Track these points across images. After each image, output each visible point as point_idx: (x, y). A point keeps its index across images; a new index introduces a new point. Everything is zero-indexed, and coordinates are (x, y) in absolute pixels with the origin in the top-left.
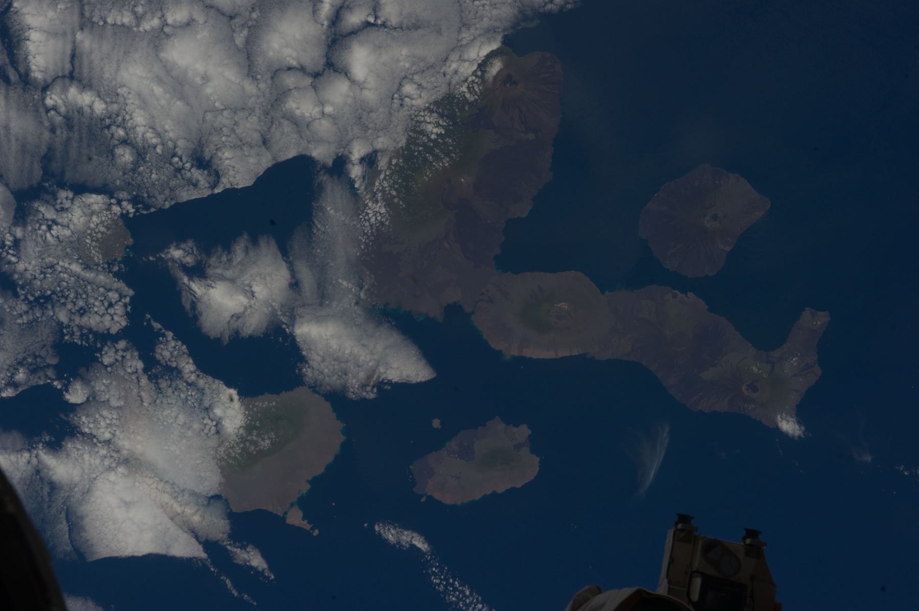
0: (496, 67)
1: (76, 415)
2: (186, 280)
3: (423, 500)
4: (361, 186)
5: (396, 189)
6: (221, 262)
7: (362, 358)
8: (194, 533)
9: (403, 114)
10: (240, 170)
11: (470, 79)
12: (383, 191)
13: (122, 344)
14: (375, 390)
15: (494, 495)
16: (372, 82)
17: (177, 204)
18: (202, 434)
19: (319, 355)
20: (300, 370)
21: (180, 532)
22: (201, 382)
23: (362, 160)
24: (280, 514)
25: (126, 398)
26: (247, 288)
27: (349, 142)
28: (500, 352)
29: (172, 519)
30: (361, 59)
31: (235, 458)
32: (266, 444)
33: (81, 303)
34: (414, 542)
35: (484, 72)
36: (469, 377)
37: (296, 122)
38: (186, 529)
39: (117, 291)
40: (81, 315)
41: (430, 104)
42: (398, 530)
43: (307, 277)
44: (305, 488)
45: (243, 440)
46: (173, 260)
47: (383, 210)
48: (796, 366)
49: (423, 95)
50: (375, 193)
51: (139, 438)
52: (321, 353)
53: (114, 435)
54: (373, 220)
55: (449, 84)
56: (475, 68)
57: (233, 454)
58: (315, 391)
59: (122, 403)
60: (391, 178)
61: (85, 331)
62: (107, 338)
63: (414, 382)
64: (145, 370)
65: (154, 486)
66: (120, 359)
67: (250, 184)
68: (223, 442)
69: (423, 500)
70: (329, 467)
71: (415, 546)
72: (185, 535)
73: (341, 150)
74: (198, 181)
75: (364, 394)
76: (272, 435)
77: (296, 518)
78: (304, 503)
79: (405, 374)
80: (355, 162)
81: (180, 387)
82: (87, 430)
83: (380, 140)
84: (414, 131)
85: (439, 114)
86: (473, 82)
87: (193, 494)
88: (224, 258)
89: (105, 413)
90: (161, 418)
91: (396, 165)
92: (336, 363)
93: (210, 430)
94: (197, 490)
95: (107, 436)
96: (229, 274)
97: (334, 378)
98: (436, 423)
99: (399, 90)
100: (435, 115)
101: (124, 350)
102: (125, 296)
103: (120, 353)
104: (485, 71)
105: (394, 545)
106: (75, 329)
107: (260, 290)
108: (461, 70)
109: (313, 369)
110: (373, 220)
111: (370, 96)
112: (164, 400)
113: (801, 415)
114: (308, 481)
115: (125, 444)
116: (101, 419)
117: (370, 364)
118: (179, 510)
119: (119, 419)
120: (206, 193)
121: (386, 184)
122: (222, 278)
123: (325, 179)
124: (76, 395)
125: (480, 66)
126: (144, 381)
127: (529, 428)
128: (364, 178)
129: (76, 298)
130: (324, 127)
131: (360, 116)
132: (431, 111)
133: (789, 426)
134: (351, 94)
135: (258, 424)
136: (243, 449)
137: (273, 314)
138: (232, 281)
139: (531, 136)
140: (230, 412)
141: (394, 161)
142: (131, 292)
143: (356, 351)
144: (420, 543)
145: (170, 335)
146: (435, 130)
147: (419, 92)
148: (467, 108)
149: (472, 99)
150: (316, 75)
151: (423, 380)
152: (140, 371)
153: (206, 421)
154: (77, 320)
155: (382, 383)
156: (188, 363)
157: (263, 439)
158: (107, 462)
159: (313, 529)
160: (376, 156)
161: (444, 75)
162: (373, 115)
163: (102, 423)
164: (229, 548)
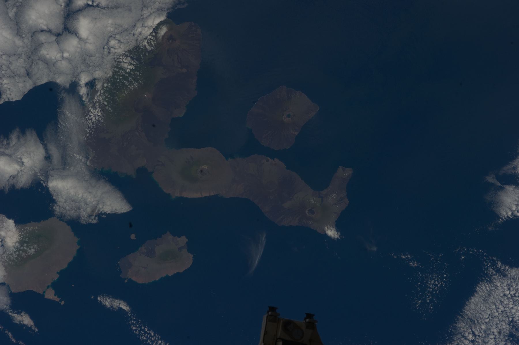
3: (126, 281)
4: (86, 99)
5: (106, 101)
9: (110, 58)
11: (149, 37)
12: (99, 102)
14: (97, 218)
15: (167, 277)
16: (91, 39)
19: (63, 198)
20: (52, 208)
23: (87, 84)
24: (41, 292)
27: (79, 74)
28: (169, 194)
32: (32, 251)
34: (121, 306)
35: (156, 33)
36: (152, 210)
37: (46, 62)
41: (126, 52)
42: (111, 299)
44: (56, 277)
47: (99, 114)
48: (335, 199)
49: (121, 46)
50: (95, 104)
52: (64, 197)
54: (94, 119)
55: (137, 40)
58: (61, 220)
60: (104, 94)
63: (120, 213)
69: (126, 281)
70: (70, 264)
71: (121, 308)
73: (74, 78)
75: (90, 220)
76: (36, 246)
77: (50, 295)
78: (55, 286)
79: (114, 209)
80: (83, 85)
83: (97, 72)
84: (117, 67)
85: (131, 57)
86: (150, 39)
91: (107, 87)
92: (73, 203)
97: (73, 212)
98: (133, 237)
99: (107, 44)
104: (157, 33)
105: (109, 308)
108: (143, 32)
109: (60, 207)
110: (94, 119)
111: (90, 47)
113: (338, 227)
114: (58, 273)
117: (94, 203)
123: (65, 95)
127: (186, 237)
128: (88, 94)
130: (64, 65)
131: (85, 59)
132: (127, 56)
133: (332, 233)
134: (79, 46)
137: (35, 174)
139: (184, 70)
141: (106, 85)
143: (85, 195)
144: (125, 307)
146: (129, 67)
147: (119, 45)
148: (147, 54)
149: (150, 49)
150: (58, 35)
151: (125, 212)
155: (101, 214)
159: (61, 301)
160: (95, 82)
161: (134, 35)
162: (92, 58)
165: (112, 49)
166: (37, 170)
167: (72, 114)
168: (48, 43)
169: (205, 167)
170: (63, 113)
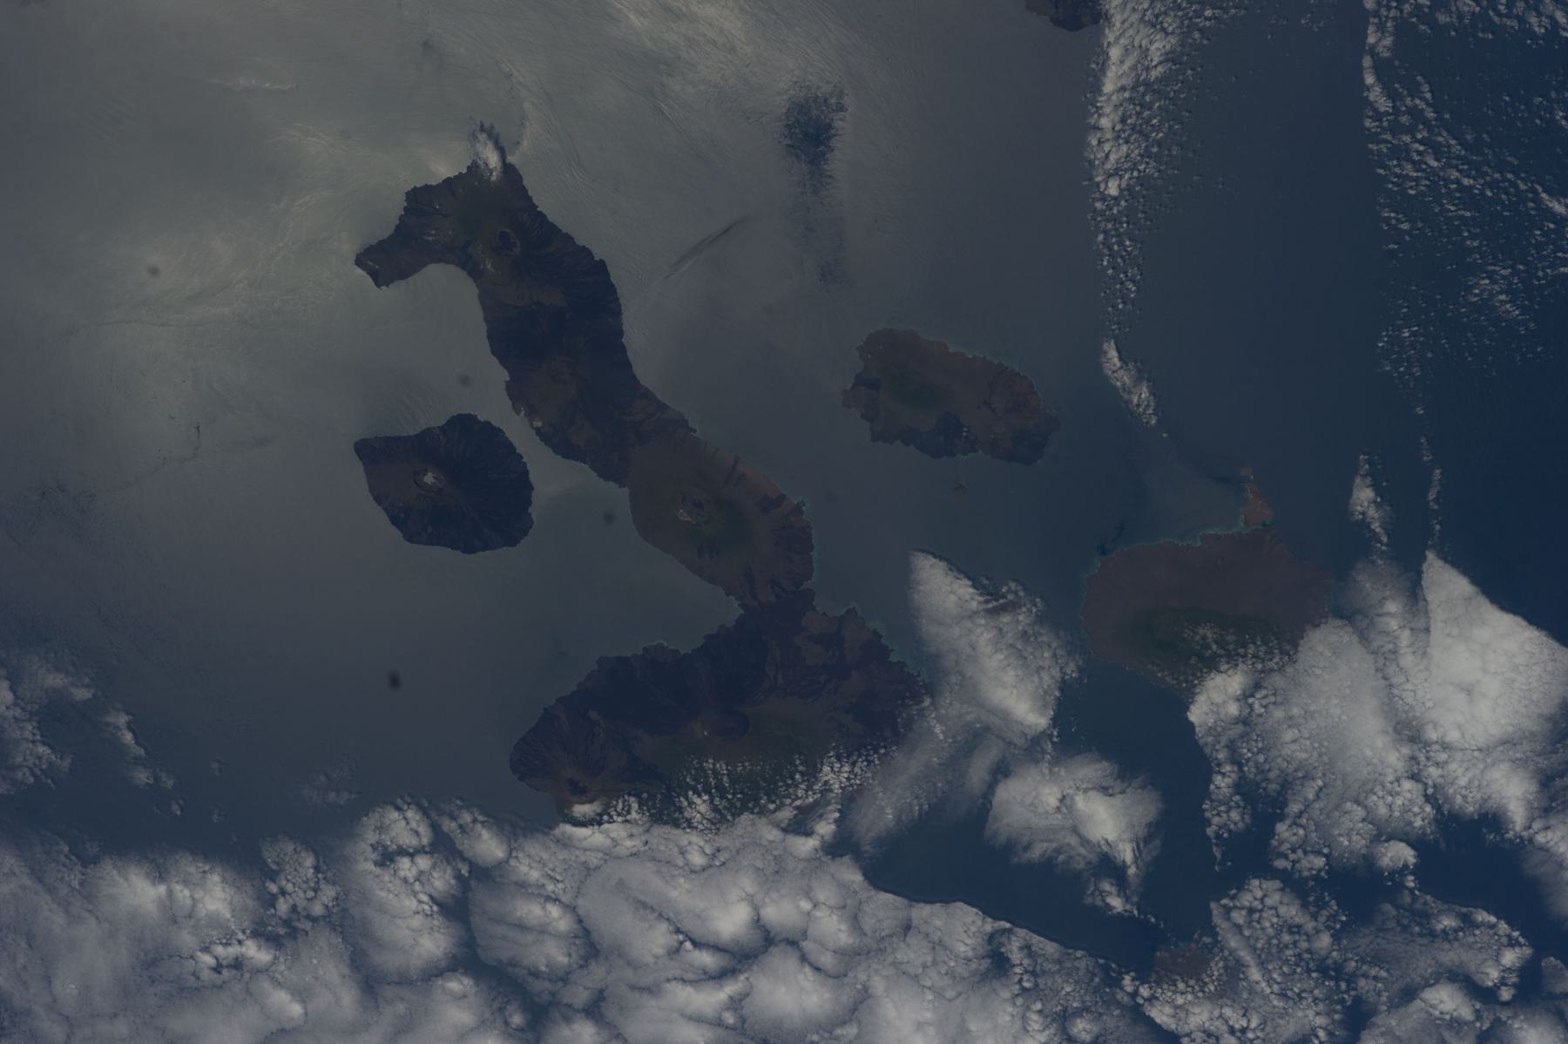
0: (582, 810)
1: (1424, 834)
2: (1132, 871)
5: (793, 778)
7: (987, 636)
8: (1414, 594)
9: (722, 841)
10: (962, 927)
13: (1280, 864)
17: (1067, 947)
18: (1279, 700)
21: (1432, 607)
22: (1221, 756)
23: (809, 834)
25: (1337, 807)
26: (1064, 810)
29: (1427, 630)
30: (731, 921)
31: (1266, 644)
32: (1207, 632)
33: (1286, 938)
35: (601, 815)
37: (855, 922)
38: (1421, 604)
39: (1228, 919)
40: (1299, 926)
43: (977, 773)
45: (1233, 658)
46: (1127, 899)
47: (826, 769)
51: (1368, 752)
52: (1036, 679)
53: (1398, 780)
54: (847, 768)
55: (647, 831)
56: (606, 826)
57: (1263, 649)
61: (1313, 909)
62: (1294, 884)
63: (943, 564)
64: (1282, 818)
65: (1409, 686)
66: (1300, 853)
67: (960, 904)
68: (1262, 671)
71: (1120, 358)
72: (1430, 597)
74: (1021, 949)
79: (950, 579)
82: (1428, 809)
86: (619, 815)
87: (1364, 638)
88: (1061, 857)
89: (1383, 811)
90: (1315, 754)
93: (1265, 697)
94: (1355, 639)
95: (1407, 785)
97: (1044, 639)
101: (1286, 857)
102: (1224, 906)
103: (1292, 857)
106: (1322, 919)
107: (1050, 796)
108: (624, 834)
111: (748, 884)
115: (1394, 760)
116: (1396, 808)
118: (1406, 634)
119: (1372, 791)
120: (1021, 932)
121: (800, 793)
122: (1085, 842)
124: (1399, 854)
125: (600, 824)
126: (1294, 808)
128: (821, 816)
129: (1286, 947)
131: (776, 872)
135: (1193, 660)
137: (1056, 761)
138: (1075, 830)
139: (594, 715)
141: (772, 807)
142: (1213, 905)
143: (988, 650)
145: (1210, 831)
146: (698, 801)
149: (632, 799)
150: (793, 943)
152: (1288, 822)
153: (1258, 709)
154: (1310, 926)
157: (1204, 638)
158: (1443, 756)
162: (759, 864)
163: (1399, 802)
164: (1385, 539)
166: (1045, 768)
167: (882, 809)
168: (822, 944)
169: (683, 515)
170: (898, 819)
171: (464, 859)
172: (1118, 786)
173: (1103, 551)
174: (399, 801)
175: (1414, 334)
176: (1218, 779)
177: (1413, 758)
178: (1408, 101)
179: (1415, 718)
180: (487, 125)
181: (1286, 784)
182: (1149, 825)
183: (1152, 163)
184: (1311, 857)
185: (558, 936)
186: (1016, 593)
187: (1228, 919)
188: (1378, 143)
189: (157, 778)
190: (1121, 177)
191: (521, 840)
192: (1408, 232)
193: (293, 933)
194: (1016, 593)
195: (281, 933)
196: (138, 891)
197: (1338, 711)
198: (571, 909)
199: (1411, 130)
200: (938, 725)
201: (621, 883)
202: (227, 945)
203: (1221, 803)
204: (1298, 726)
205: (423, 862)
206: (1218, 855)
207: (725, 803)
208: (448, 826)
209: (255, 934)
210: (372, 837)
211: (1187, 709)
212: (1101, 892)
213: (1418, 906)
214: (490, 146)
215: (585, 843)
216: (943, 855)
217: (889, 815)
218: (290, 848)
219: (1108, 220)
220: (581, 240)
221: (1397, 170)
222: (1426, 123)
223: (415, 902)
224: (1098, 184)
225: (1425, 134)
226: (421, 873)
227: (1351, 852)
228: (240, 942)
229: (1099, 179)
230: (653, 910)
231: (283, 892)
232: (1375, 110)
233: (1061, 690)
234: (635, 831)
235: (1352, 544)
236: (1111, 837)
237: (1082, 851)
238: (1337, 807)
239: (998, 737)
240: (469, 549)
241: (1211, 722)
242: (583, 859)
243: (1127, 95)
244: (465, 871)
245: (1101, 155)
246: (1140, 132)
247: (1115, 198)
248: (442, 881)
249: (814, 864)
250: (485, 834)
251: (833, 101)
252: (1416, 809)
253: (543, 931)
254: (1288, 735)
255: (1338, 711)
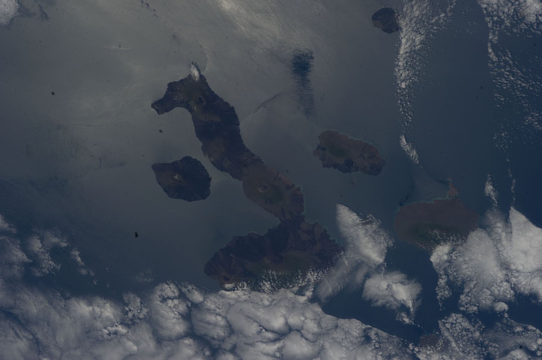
0: (228, 286)
2: (412, 310)
5: (298, 277)
6: (391, 305)
8: (507, 220)
9: (274, 297)
10: (355, 327)
13: (462, 309)
18: (461, 255)
22: (442, 273)
23: (303, 295)
30: (278, 323)
31: (456, 236)
32: (436, 232)
35: (234, 288)
37: (319, 324)
38: (509, 224)
39: (445, 326)
43: (359, 276)
45: (445, 241)
46: (410, 319)
47: (309, 274)
51: (491, 273)
52: (379, 246)
53: (502, 282)
54: (316, 274)
55: (250, 293)
57: (455, 238)
59: (485, 290)
61: (473, 324)
62: (467, 315)
63: (347, 208)
64: (462, 293)
65: (505, 251)
66: (469, 305)
67: (354, 319)
68: (455, 245)
71: (406, 141)
79: (350, 213)
81: (452, 277)
83: (291, 296)
84: (275, 289)
87: (489, 234)
88: (388, 305)
89: (496, 292)
90: (473, 273)
93: (456, 253)
94: (487, 235)
95: (505, 284)
96: (392, 299)
97: (382, 233)
100: (263, 288)
101: (464, 306)
103: (466, 306)
105: (416, 149)
106: (476, 327)
108: (242, 294)
110: (316, 274)
111: (283, 311)
112: (465, 278)
115: (500, 275)
116: (501, 291)
118: (504, 235)
119: (493, 285)
121: (300, 282)
122: (396, 300)
125: (234, 290)
126: (467, 290)
128: (307, 290)
131: (292, 307)
132: (263, 290)
135: (432, 241)
136: (449, 237)
137: (386, 273)
138: (392, 296)
139: (231, 255)
140: (440, 254)
141: (291, 286)
142: (439, 322)
143: (363, 236)
145: (438, 297)
146: (266, 284)
149: (245, 283)
152: (465, 295)
153: (454, 258)
156: (441, 283)
157: (435, 234)
162: (287, 305)
163: (502, 289)
164: (496, 202)
165: (270, 300)
166: (382, 275)
169: (260, 190)
170: (333, 291)
171: (189, 301)
172: (407, 282)
173: (401, 204)
174: (168, 282)
175: (506, 135)
176: (440, 280)
177: (507, 275)
178: (503, 58)
179: (507, 262)
180: (194, 62)
181: (463, 282)
182: (417, 295)
183: (417, 77)
184: (473, 307)
185: (221, 326)
186: (372, 218)
187: (445, 326)
188: (493, 71)
189: (89, 273)
190: (406, 82)
191: (208, 295)
192: (504, 101)
193: (134, 323)
194: (372, 218)
195: (130, 323)
196: (83, 309)
197: (481, 259)
198: (225, 318)
199: (504, 68)
200: (346, 261)
201: (241, 310)
202: (112, 327)
203: (442, 288)
204: (468, 263)
205: (176, 302)
206: (441, 305)
207: (275, 285)
208: (184, 290)
209: (121, 324)
210: (159, 293)
211: (430, 257)
212: (401, 317)
213: (509, 323)
214: (195, 69)
215: (229, 297)
216: (349, 304)
217: (330, 290)
218: (132, 296)
219: (402, 96)
220: (225, 101)
221: (500, 81)
222: (509, 65)
223: (173, 314)
224: (398, 84)
225: (509, 69)
226: (175, 305)
227: (486, 305)
228: (116, 326)
229: (399, 82)
230: (252, 319)
231: (130, 310)
232: (492, 60)
233: (387, 250)
234: (246, 293)
235: (485, 204)
236: (405, 298)
237: (395, 303)
238: (481, 290)
239: (366, 265)
240: (190, 200)
241: (438, 261)
242: (229, 302)
243: (408, 55)
244: (190, 305)
245: (399, 74)
246: (412, 67)
247: (404, 89)
248: (182, 308)
249: (305, 305)
250: (196, 293)
251: (309, 55)
252: (508, 292)
253: (216, 325)
254: (464, 266)
255: (481, 259)
